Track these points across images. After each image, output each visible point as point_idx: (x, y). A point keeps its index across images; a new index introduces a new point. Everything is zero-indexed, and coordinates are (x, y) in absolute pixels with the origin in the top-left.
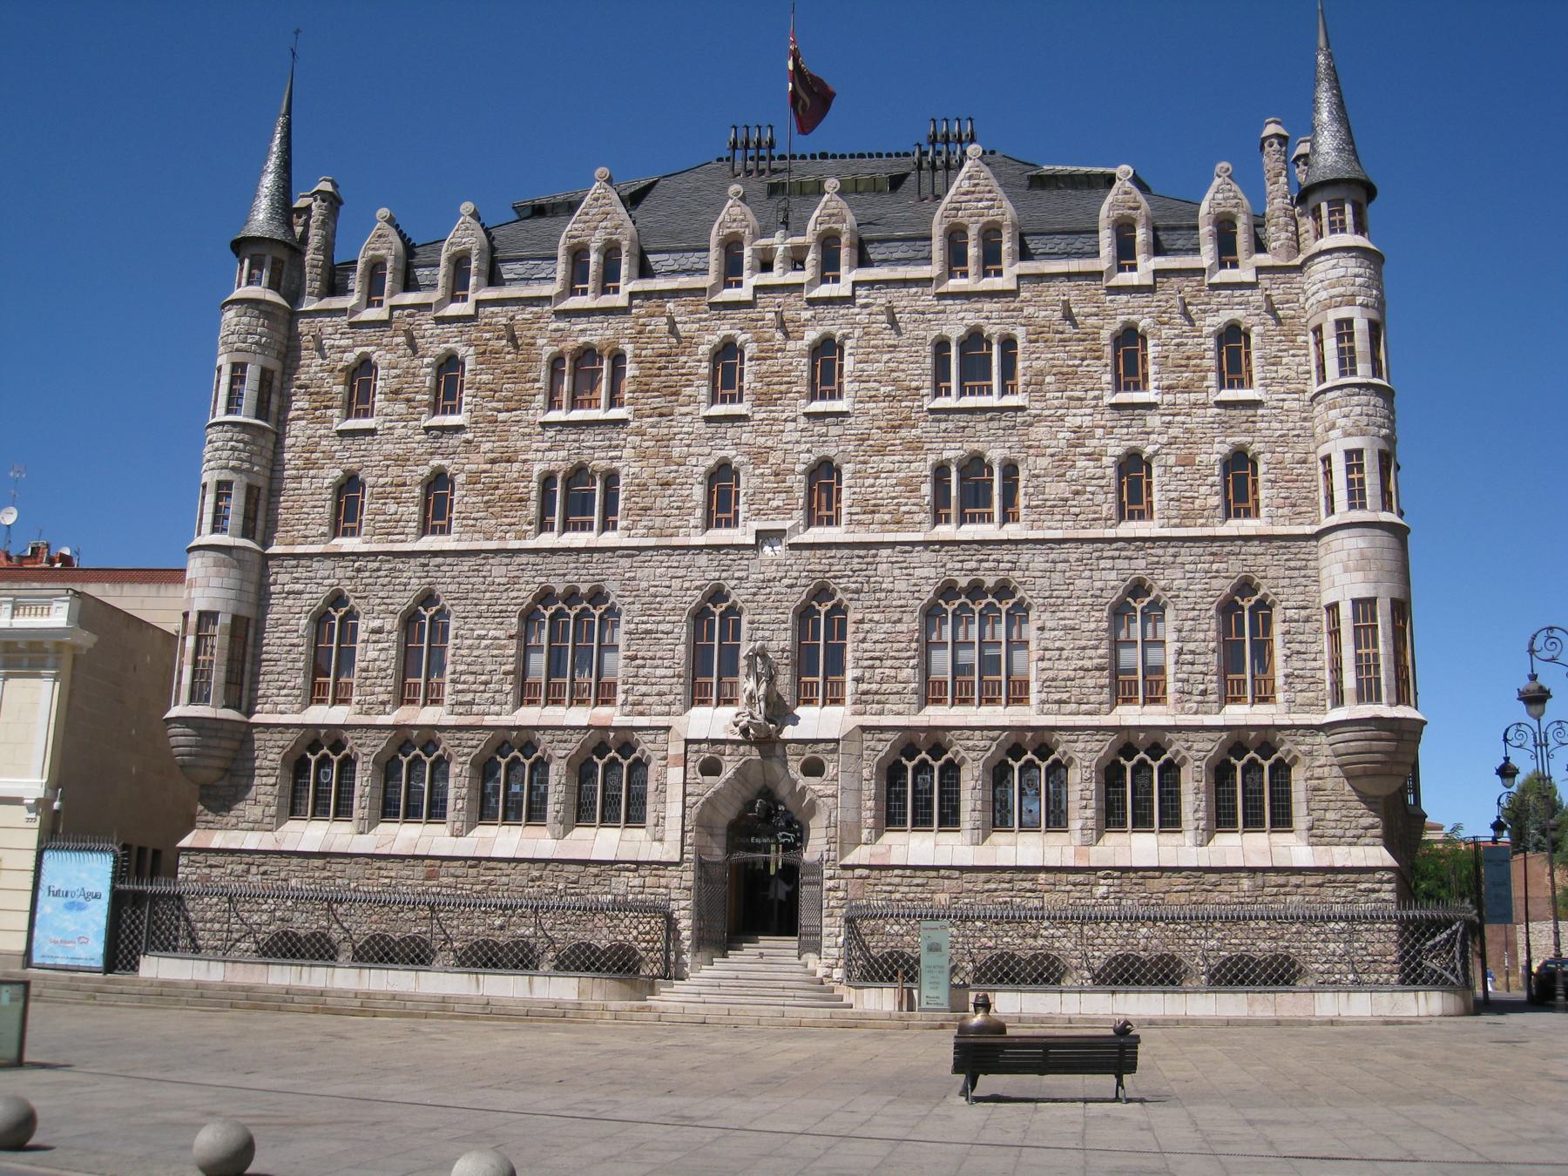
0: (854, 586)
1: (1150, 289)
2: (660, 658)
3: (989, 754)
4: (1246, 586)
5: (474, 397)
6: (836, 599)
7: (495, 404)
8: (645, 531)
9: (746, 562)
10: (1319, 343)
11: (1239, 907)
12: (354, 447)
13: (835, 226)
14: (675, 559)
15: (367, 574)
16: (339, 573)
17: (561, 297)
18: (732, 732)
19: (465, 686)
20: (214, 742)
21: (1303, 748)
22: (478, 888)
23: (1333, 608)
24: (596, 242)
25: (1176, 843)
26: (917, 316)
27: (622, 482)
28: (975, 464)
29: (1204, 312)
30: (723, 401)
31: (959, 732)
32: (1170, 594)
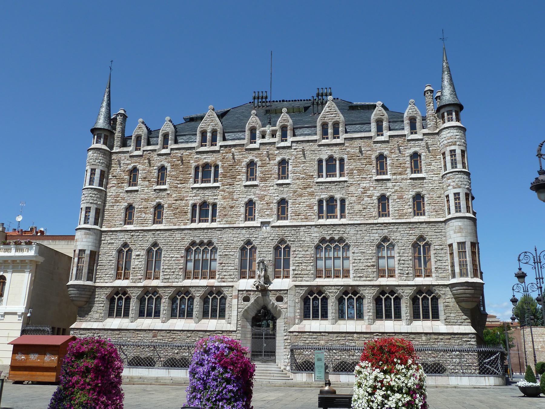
1: (387, 142)
2: (230, 263)
3: (337, 294)
4: (421, 238)
5: (170, 179)
7: (177, 182)
8: (225, 222)
9: (258, 232)
10: (444, 158)
11: (422, 346)
12: (131, 196)
13: (286, 123)
14: (235, 231)
15: (135, 237)
16: (126, 237)
17: (198, 147)
18: (253, 287)
19: (167, 273)
20: (83, 293)
21: (442, 292)
22: (170, 340)
23: (451, 245)
24: (209, 129)
25: (399, 324)
26: (312, 152)
27: (218, 206)
28: (331, 199)
29: (406, 149)
30: (250, 180)
31: (327, 287)
32: (396, 241)
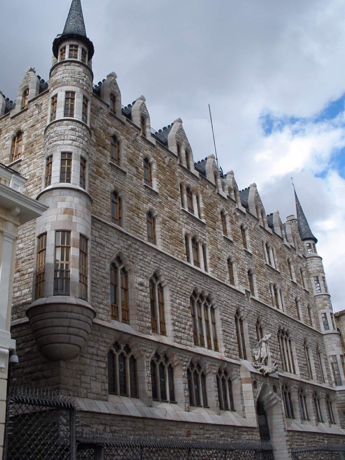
16: (122, 245)
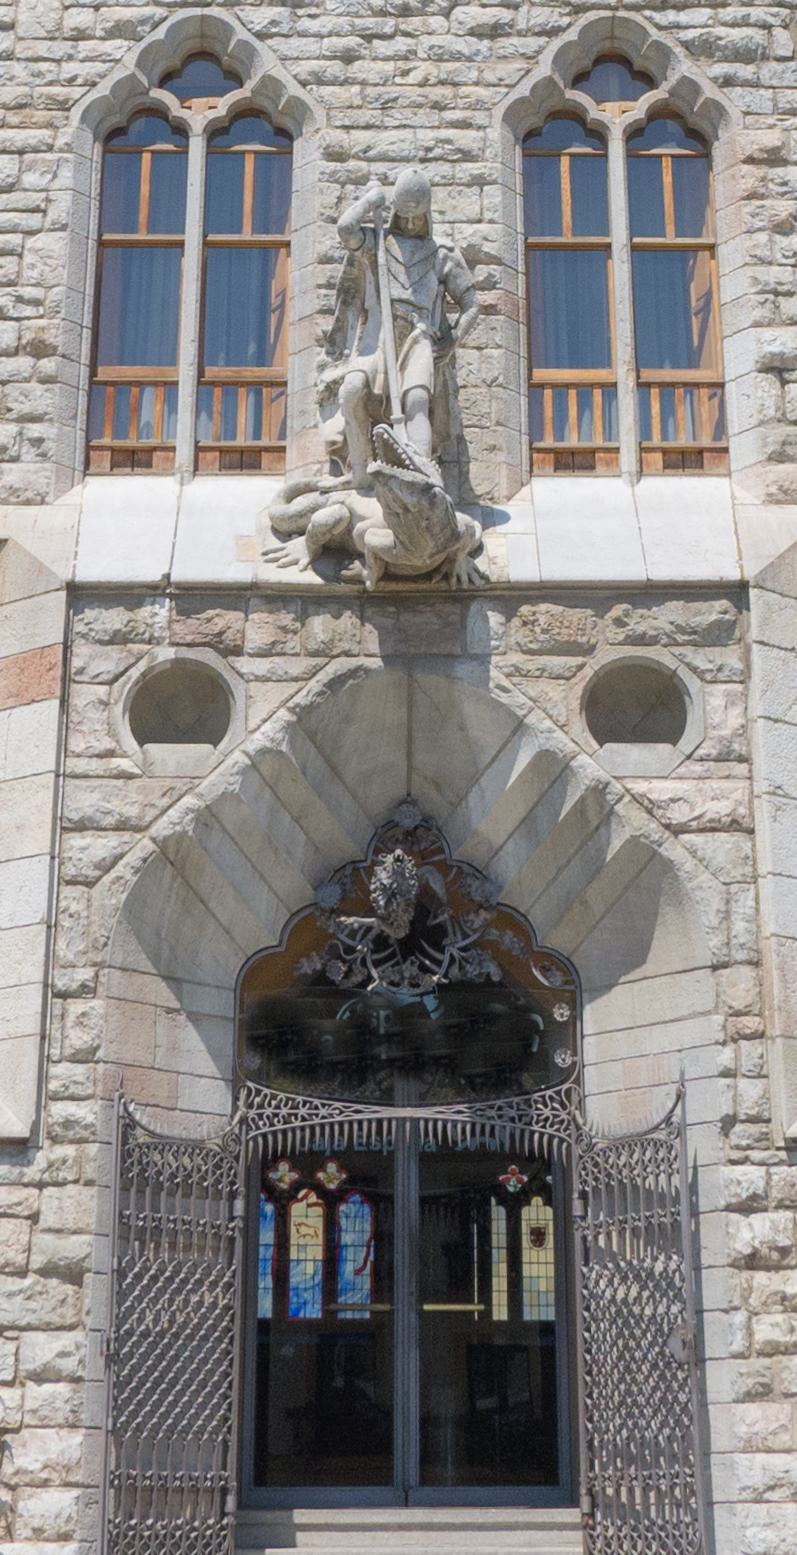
0: (736, 35)
6: (673, 78)
